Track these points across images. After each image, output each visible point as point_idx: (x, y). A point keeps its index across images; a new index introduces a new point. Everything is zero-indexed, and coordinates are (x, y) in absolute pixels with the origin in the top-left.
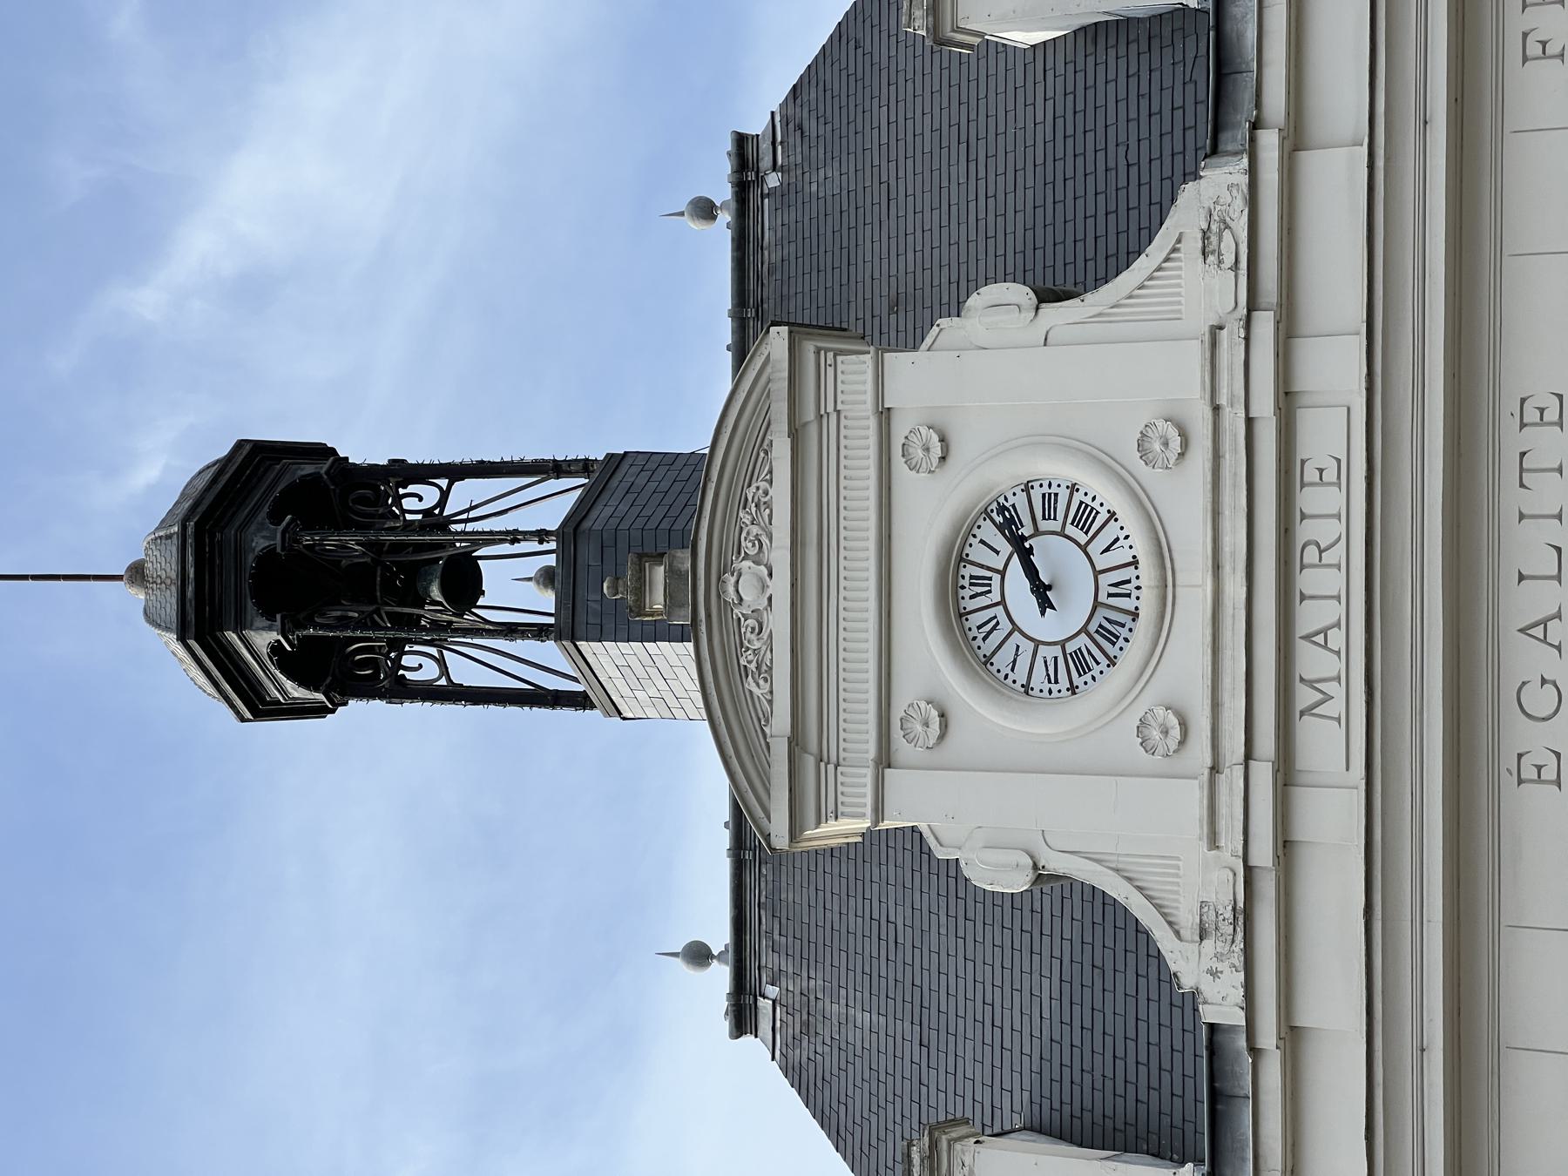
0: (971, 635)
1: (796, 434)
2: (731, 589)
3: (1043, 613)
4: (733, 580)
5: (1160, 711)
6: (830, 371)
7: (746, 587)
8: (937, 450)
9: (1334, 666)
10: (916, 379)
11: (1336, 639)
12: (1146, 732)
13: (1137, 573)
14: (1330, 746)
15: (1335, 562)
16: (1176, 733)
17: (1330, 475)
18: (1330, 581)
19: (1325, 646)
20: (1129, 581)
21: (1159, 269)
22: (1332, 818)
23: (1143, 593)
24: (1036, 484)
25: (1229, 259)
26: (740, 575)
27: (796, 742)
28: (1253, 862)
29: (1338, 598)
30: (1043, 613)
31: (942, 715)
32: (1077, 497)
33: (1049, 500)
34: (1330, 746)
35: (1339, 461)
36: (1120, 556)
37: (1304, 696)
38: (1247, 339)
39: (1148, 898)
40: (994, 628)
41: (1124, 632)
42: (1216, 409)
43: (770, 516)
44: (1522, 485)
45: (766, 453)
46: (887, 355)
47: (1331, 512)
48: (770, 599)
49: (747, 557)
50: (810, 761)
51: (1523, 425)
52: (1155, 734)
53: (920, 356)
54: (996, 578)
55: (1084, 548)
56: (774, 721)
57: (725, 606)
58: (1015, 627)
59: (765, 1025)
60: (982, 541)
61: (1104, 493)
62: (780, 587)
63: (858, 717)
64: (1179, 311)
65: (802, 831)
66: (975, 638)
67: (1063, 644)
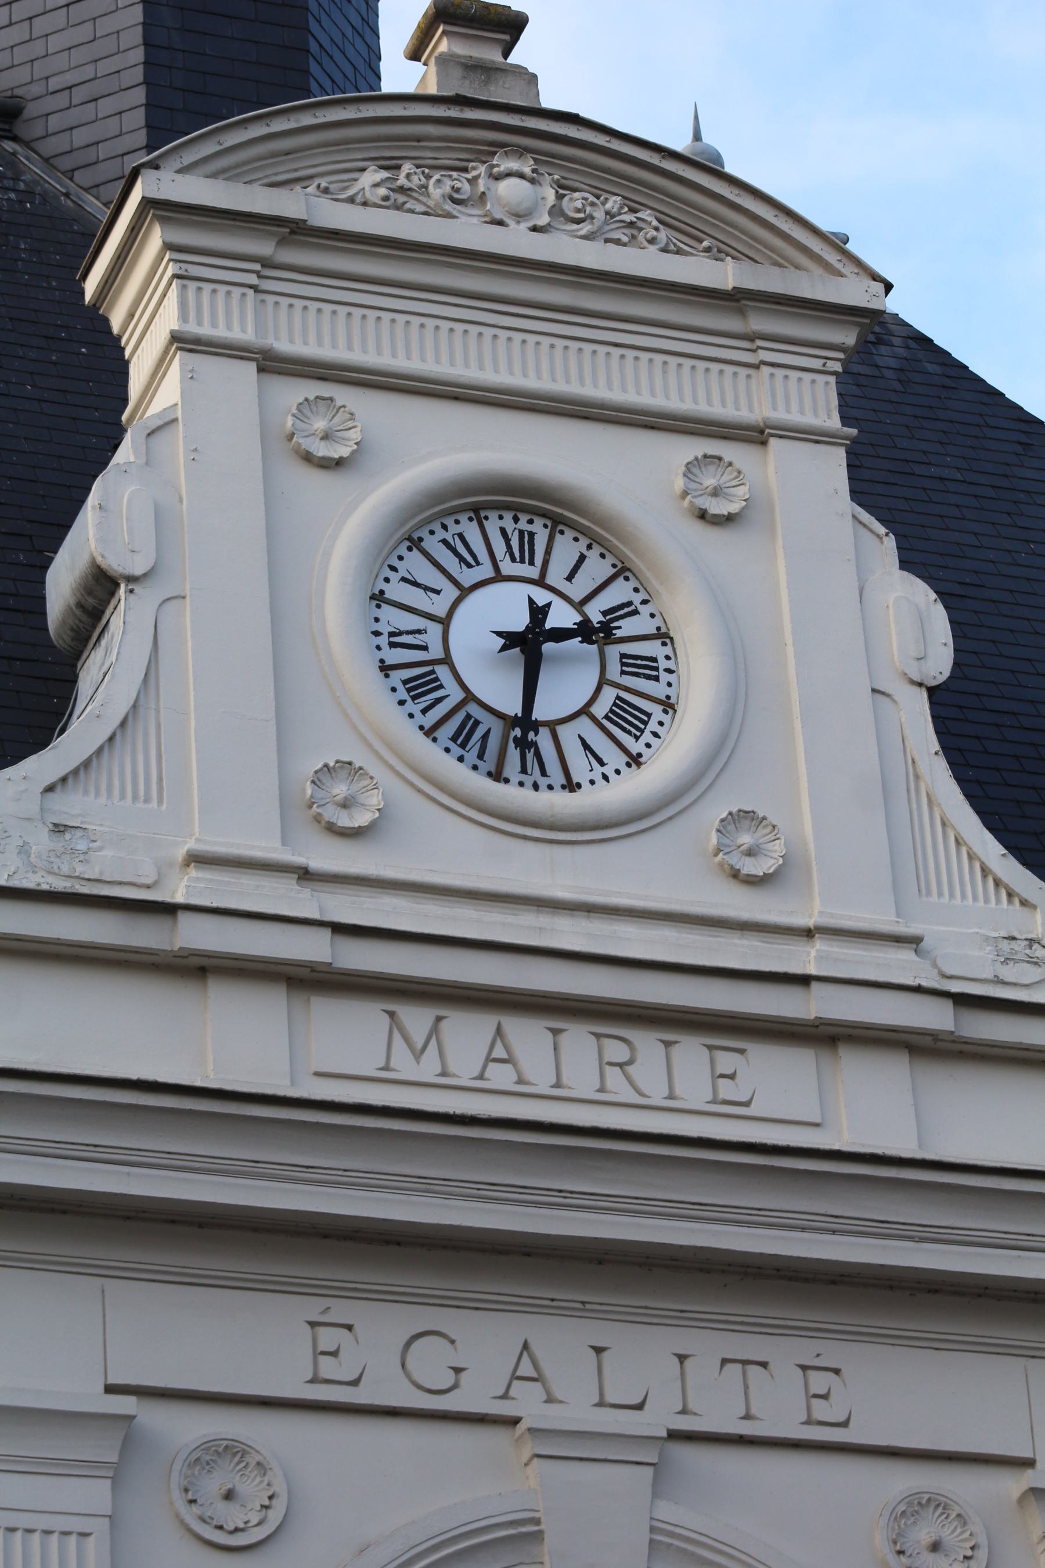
0: (449, 521)
1: (736, 299)
2: (513, 165)
3: (499, 634)
4: (527, 171)
5: (374, 799)
6: (817, 364)
8: (717, 507)
9: (465, 1070)
11: (501, 1076)
12: (343, 774)
13: (557, 786)
14: (345, 1051)
15: (609, 1084)
16: (344, 820)
17: (727, 1090)
19: (489, 1059)
20: (544, 773)
21: (985, 871)
22: (238, 1043)
23: (528, 793)
24: (668, 650)
25: (1008, 973)
26: (532, 181)
27: (295, 231)
28: (183, 917)
29: (386, 1068)
30: (499, 634)
31: (339, 463)
32: (656, 710)
33: (647, 668)
34: (345, 1051)
35: (747, 1104)
36: (580, 766)
37: (417, 1018)
38: (918, 990)
39: (99, 751)
40: (462, 559)
41: (471, 756)
42: (808, 933)
43: (618, 242)
44: (725, 1361)
45: (708, 250)
46: (842, 453)
47: (672, 1086)
48: (500, 223)
49: (560, 197)
50: (265, 248)
51: (804, 1368)
52: (340, 789)
53: (844, 502)
54: (534, 572)
55: (585, 711)
56: (324, 202)
57: (487, 152)
58: (465, 592)
60: (582, 558)
61: (674, 750)
62: (516, 241)
63: (400, 343)
64: (929, 893)
65: (163, 220)
66: (445, 527)
67: (447, 660)
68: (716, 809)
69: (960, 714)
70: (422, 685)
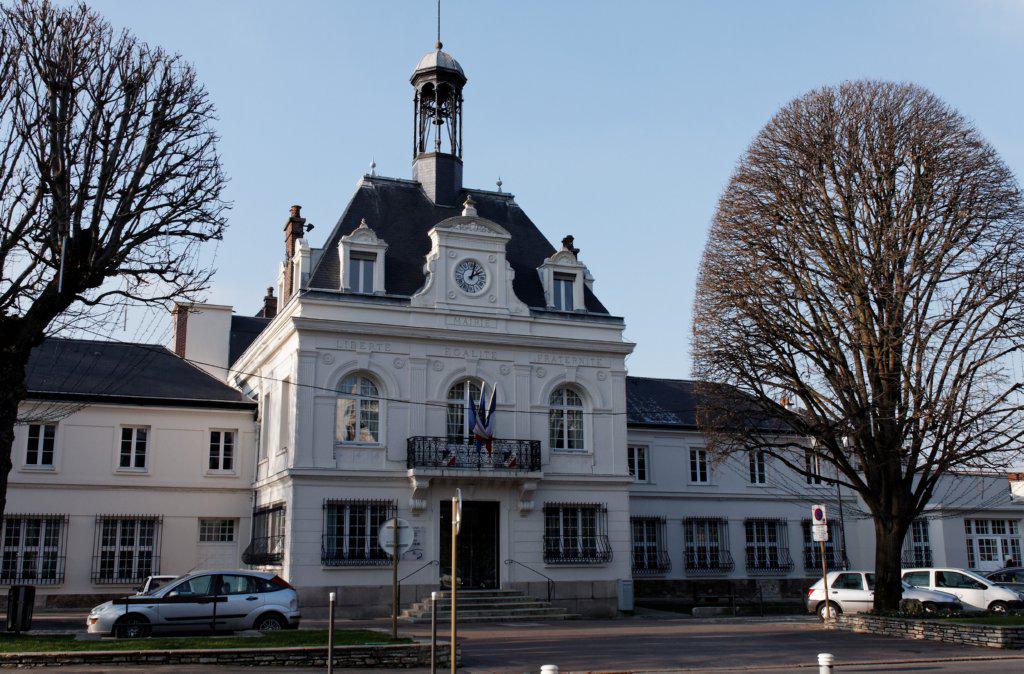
7: (473, 226)
10: (501, 258)
18: (473, 324)
33: (482, 278)
59: (366, 183)
61: (485, 287)
62: (473, 233)
68: (489, 295)
69: (515, 283)
70: (460, 281)
